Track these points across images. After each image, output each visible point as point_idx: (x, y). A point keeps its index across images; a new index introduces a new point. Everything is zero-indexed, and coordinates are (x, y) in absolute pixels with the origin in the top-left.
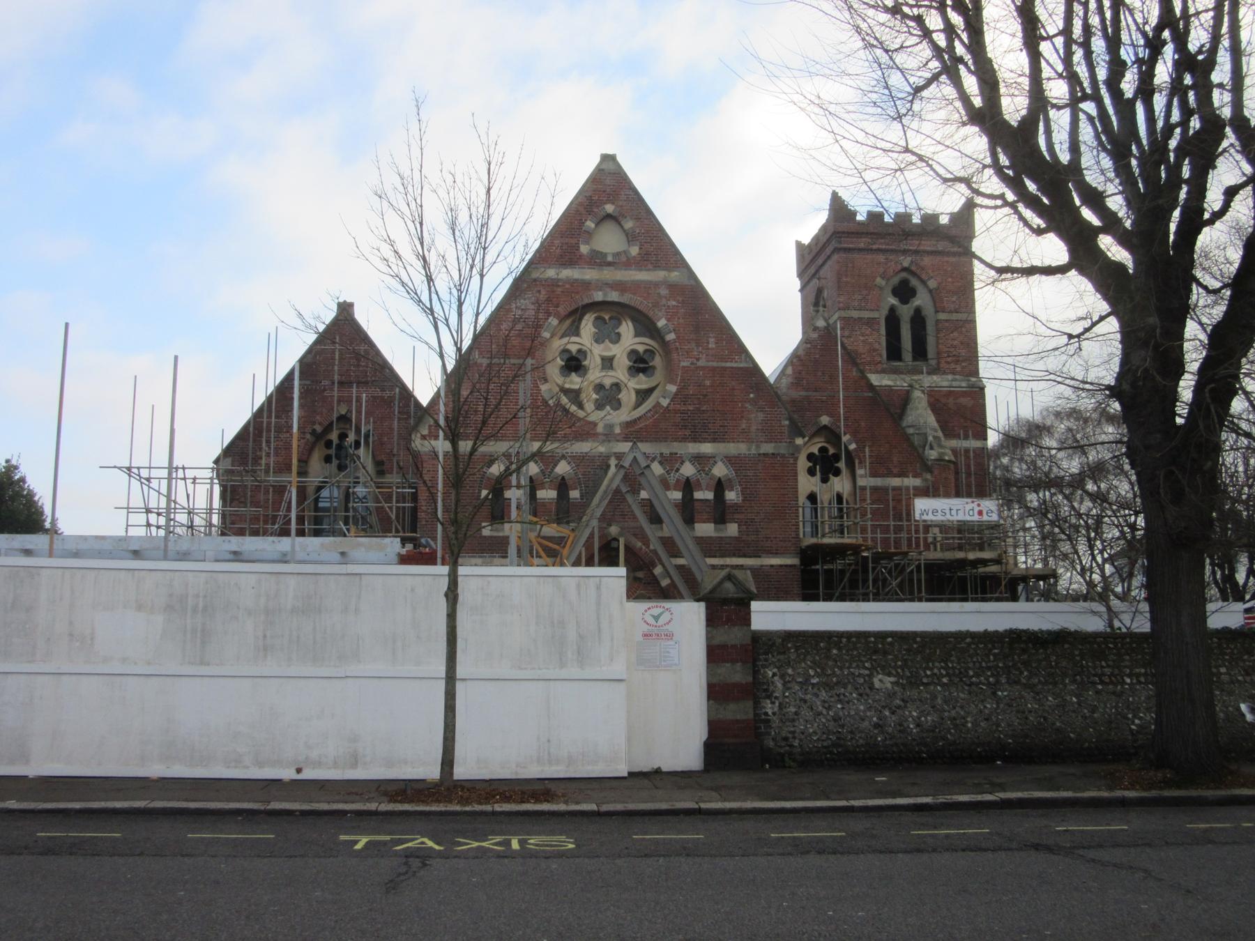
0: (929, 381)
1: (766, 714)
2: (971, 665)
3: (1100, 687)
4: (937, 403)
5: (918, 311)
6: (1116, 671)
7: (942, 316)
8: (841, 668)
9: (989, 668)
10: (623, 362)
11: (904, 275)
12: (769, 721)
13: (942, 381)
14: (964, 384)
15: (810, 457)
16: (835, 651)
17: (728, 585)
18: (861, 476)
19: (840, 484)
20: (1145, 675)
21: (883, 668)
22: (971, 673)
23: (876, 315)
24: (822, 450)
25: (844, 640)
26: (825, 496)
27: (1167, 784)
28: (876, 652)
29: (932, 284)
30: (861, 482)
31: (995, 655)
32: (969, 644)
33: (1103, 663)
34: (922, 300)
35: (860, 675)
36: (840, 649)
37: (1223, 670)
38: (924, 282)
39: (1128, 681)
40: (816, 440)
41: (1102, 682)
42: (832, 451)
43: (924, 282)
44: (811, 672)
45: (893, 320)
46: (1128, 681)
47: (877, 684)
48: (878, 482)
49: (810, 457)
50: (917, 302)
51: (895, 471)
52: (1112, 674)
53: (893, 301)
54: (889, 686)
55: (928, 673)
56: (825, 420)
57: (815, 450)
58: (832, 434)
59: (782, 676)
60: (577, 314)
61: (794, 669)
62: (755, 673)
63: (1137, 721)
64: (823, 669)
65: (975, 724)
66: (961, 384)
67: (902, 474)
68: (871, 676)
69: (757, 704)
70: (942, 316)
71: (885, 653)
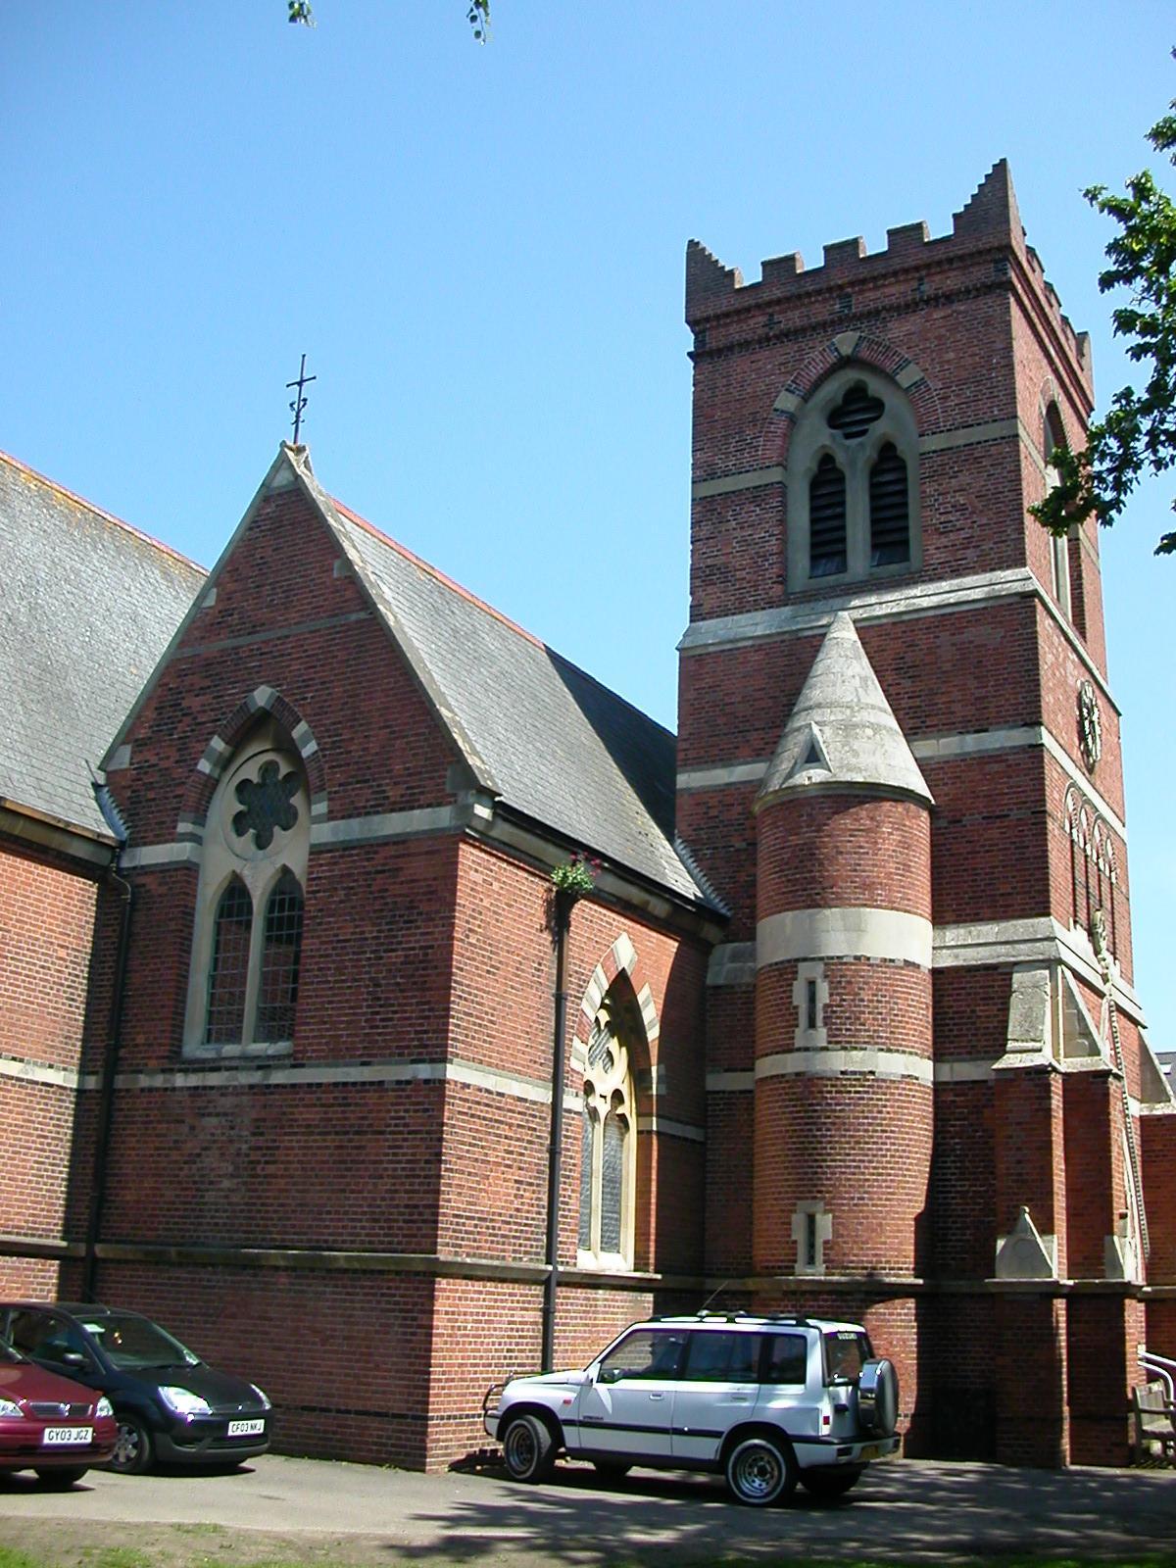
4: (895, 653)
5: (888, 452)
11: (850, 376)
19: (291, 851)
24: (268, 769)
29: (905, 379)
34: (897, 423)
38: (890, 379)
43: (890, 379)
45: (827, 480)
48: (353, 829)
49: (243, 787)
50: (880, 428)
51: (393, 793)
67: (407, 805)
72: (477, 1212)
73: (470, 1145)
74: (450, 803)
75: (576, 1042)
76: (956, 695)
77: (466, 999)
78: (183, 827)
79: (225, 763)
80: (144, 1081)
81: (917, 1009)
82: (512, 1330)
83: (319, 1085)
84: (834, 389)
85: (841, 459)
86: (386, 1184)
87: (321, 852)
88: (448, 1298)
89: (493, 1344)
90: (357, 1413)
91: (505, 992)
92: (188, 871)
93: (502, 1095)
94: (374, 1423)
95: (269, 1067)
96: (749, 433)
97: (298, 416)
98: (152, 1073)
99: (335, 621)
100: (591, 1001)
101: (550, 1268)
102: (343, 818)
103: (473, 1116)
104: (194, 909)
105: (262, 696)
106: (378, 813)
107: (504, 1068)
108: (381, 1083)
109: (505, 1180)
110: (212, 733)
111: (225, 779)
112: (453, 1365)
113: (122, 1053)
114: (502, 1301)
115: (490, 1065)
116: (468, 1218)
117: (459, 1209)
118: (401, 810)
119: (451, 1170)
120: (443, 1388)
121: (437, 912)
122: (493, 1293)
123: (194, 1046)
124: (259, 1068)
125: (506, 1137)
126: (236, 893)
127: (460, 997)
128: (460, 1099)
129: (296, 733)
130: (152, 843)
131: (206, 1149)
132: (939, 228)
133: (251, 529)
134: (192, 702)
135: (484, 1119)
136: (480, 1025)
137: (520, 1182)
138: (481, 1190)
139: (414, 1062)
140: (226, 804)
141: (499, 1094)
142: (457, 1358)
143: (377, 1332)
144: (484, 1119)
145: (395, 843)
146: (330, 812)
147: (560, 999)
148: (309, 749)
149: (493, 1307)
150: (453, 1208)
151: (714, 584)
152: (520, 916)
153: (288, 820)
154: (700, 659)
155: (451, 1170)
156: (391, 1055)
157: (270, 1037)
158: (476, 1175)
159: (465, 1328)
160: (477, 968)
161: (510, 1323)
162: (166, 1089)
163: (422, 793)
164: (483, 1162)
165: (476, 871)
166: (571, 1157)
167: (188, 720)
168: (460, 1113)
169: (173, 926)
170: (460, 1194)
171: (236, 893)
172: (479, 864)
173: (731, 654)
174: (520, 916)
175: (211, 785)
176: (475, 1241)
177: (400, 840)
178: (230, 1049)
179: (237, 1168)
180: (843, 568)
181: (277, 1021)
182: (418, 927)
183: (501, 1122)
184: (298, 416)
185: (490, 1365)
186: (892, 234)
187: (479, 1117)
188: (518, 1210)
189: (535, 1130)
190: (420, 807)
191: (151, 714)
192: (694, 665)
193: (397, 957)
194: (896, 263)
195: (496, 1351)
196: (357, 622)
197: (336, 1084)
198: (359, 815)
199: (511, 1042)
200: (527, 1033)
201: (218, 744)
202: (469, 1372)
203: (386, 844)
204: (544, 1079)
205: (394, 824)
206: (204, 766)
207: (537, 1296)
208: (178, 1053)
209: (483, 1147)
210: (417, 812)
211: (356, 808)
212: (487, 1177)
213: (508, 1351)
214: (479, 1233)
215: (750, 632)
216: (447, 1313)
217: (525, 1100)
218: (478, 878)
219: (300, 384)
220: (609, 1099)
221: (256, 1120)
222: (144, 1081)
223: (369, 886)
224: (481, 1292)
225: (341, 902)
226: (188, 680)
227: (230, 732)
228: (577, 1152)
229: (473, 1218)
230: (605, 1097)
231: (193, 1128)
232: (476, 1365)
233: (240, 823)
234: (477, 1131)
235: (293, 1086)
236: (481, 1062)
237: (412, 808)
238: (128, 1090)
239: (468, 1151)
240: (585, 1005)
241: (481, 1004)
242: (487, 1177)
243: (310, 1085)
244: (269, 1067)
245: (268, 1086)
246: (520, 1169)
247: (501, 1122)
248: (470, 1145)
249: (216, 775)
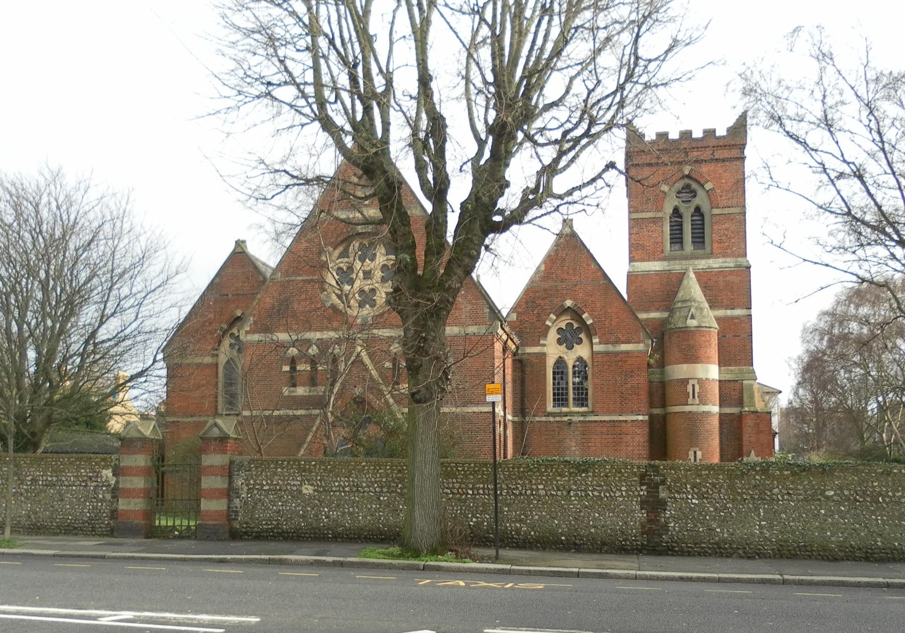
0: (702, 264)
1: (236, 507)
2: (364, 480)
3: (451, 496)
4: (707, 280)
5: (698, 209)
6: (464, 486)
7: (716, 211)
8: (282, 481)
9: (376, 482)
10: (378, 274)
11: (687, 181)
12: (237, 512)
13: (715, 263)
14: (732, 265)
15: (560, 330)
16: (279, 470)
17: (215, 430)
18: (596, 344)
19: (582, 350)
20: (483, 489)
21: (308, 481)
22: (364, 485)
23: (660, 215)
25: (285, 463)
26: (570, 359)
27: (392, 556)
28: (304, 471)
29: (708, 186)
30: (597, 348)
31: (380, 474)
32: (364, 467)
33: (454, 480)
34: (701, 199)
35: (294, 485)
36: (283, 468)
37: (541, 487)
39: (471, 492)
40: (563, 318)
41: (452, 493)
42: (576, 326)
43: (702, 186)
44: (264, 483)
46: (471, 492)
47: (305, 491)
48: (610, 348)
49: (560, 330)
50: (697, 201)
52: (460, 487)
53: (676, 202)
54: (311, 492)
55: (337, 484)
56: (569, 303)
57: (563, 326)
58: (576, 313)
59: (247, 485)
60: (348, 240)
61: (255, 481)
62: (230, 483)
63: (474, 520)
64: (272, 481)
65: (365, 517)
66: (730, 263)
67: (628, 342)
68: (301, 485)
69: (230, 501)
70: (716, 211)
71: (310, 472)
80: (537, 419)
81: (715, 392)
123: (550, 408)
126: (560, 363)
132: (721, 132)
140: (553, 335)
148: (589, 322)
157: (578, 406)
171: (560, 363)
173: (647, 275)
177: (627, 352)
178: (564, 409)
180: (682, 248)
181: (581, 400)
186: (705, 131)
191: (524, 305)
194: (705, 144)
201: (553, 317)
205: (624, 347)
215: (654, 268)
222: (537, 419)
226: (537, 294)
233: (560, 342)
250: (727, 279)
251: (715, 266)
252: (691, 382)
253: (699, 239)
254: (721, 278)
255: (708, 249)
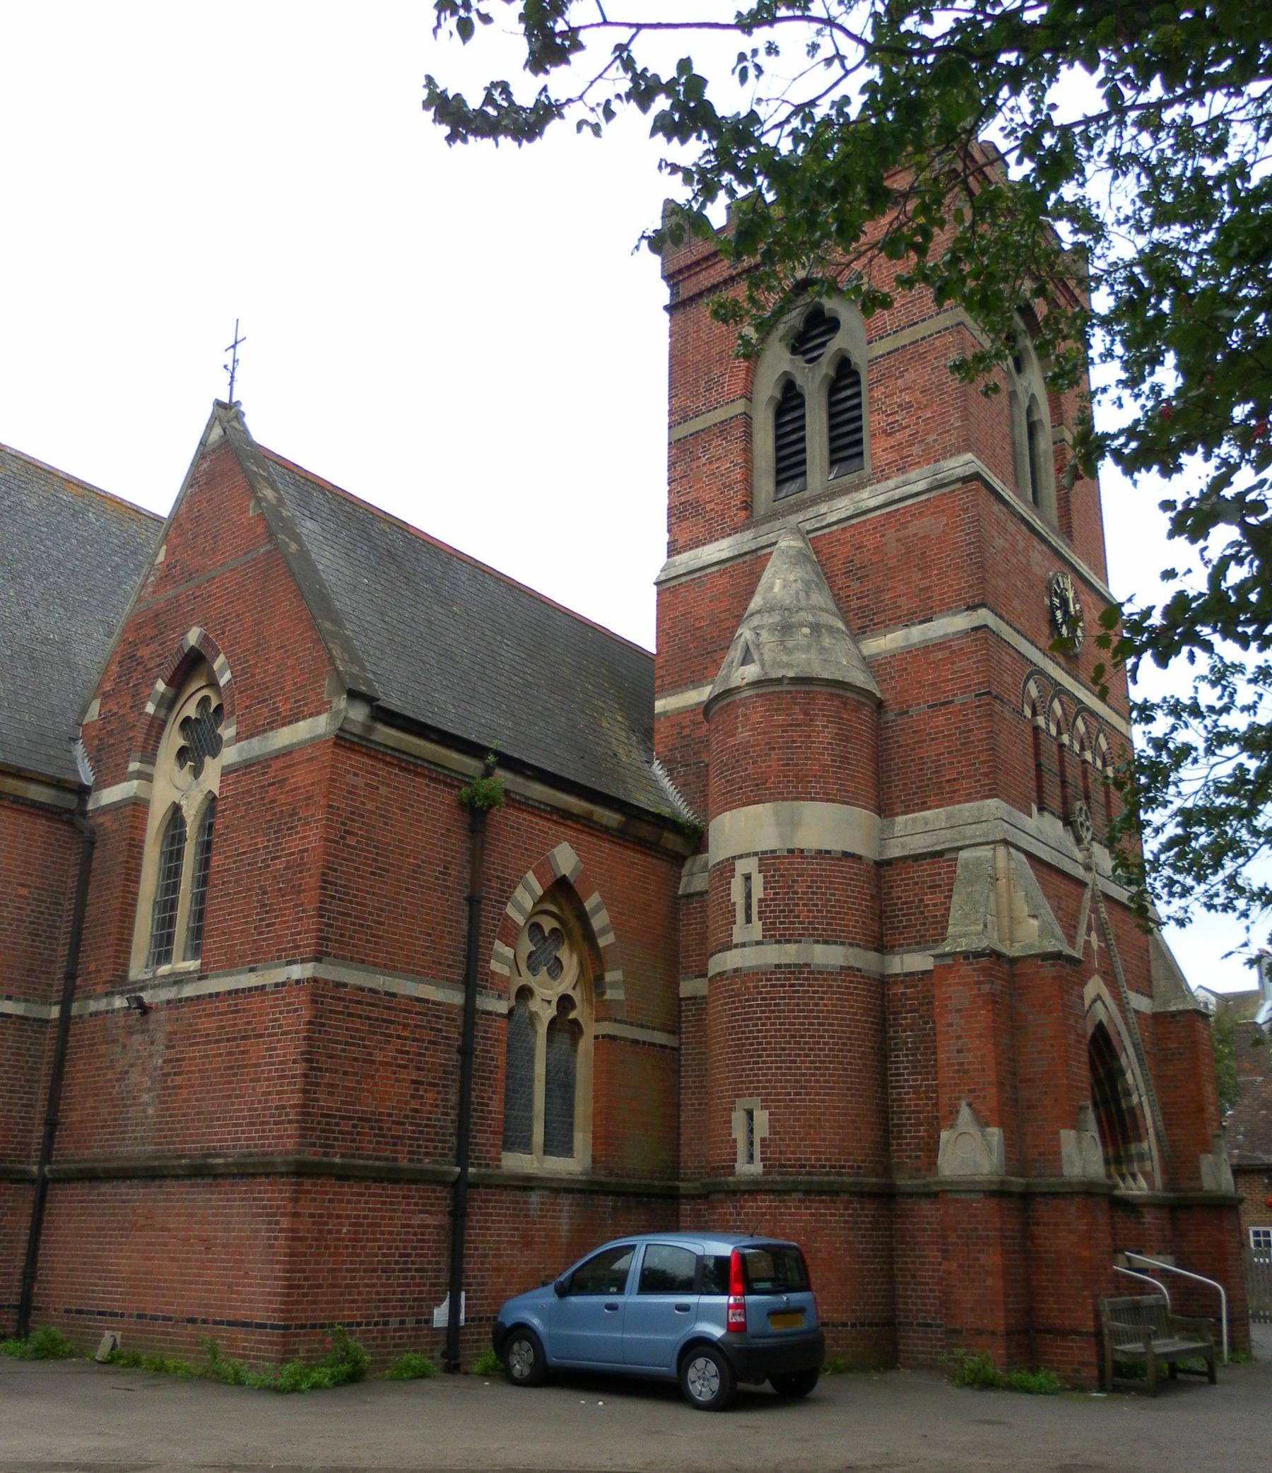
45: (789, 400)
72: (356, 1111)
73: (347, 1043)
74: (326, 710)
75: (499, 946)
76: (902, 589)
77: (340, 899)
78: (134, 766)
79: (169, 703)
80: (93, 1006)
82: (408, 1233)
83: (218, 994)
84: (794, 319)
85: (799, 381)
86: (261, 1087)
87: (230, 773)
88: (314, 1200)
89: (380, 1248)
90: (230, 1323)
91: (398, 893)
92: (138, 806)
93: (394, 995)
94: (240, 1333)
95: (181, 981)
96: (716, 371)
97: (232, 377)
98: (98, 998)
99: (249, 557)
100: (520, 908)
101: (458, 1169)
102: (247, 738)
103: (350, 1015)
104: (143, 841)
105: (193, 637)
106: (272, 729)
107: (395, 968)
108: (264, 986)
109: (397, 1080)
110: (157, 677)
111: (171, 720)
112: (321, 1271)
113: (79, 981)
114: (392, 1203)
115: (375, 964)
116: (343, 1118)
117: (330, 1108)
118: (290, 723)
119: (320, 1070)
120: (305, 1295)
121: (313, 815)
122: (380, 1195)
123: (137, 972)
124: (175, 983)
125: (399, 1037)
127: (333, 897)
128: (332, 998)
129: (216, 666)
130: (110, 785)
131: (132, 1066)
133: (192, 486)
134: (144, 652)
135: (368, 1018)
136: (361, 926)
137: (421, 1083)
138: (362, 1090)
139: (289, 963)
140: (173, 740)
141: (387, 994)
142: (325, 1263)
143: (248, 1238)
144: (368, 1018)
145: (285, 755)
146: (238, 734)
147: (473, 901)
149: (380, 1210)
150: (322, 1108)
151: (687, 520)
152: (417, 821)
153: (215, 747)
154: (674, 591)
155: (320, 1070)
156: (273, 958)
158: (355, 1074)
159: (339, 1232)
160: (357, 869)
161: (404, 1226)
162: (107, 1012)
163: (306, 704)
164: (365, 1061)
165: (356, 775)
166: (492, 1059)
167: (140, 668)
168: (331, 1012)
169: (121, 859)
170: (330, 1094)
172: (361, 769)
174: (417, 821)
175: (157, 728)
176: (353, 1141)
177: (287, 752)
178: (164, 969)
179: (153, 1083)
182: (297, 833)
183: (393, 1022)
184: (232, 377)
185: (375, 1270)
187: (360, 1017)
188: (416, 1111)
189: (440, 1030)
190: (304, 718)
192: (668, 589)
193: (279, 865)
195: (384, 1255)
196: (264, 554)
197: (230, 992)
198: (258, 733)
199: (406, 943)
200: (429, 935)
202: (345, 1278)
203: (277, 757)
204: (453, 981)
206: (150, 708)
207: (445, 1199)
208: (124, 977)
209: (365, 1046)
210: (301, 723)
211: (257, 727)
212: (372, 1077)
213: (401, 1255)
214: (358, 1133)
216: (312, 1216)
217: (427, 1001)
218: (360, 782)
219: (234, 347)
220: (554, 1004)
221: (171, 1033)
222: (93, 1006)
223: (263, 799)
224: (362, 1195)
225: (242, 817)
226: (142, 632)
227: (169, 674)
228: (500, 1054)
229: (351, 1118)
230: (549, 1002)
231: (124, 1046)
232: (353, 1270)
234: (357, 1030)
235: (198, 997)
236: (363, 962)
237: (298, 720)
238: (81, 1016)
239: (344, 1050)
240: (510, 910)
241: (364, 905)
242: (372, 1077)
243: (211, 995)
244: (181, 981)
245: (180, 1000)
246: (419, 1069)
247: (393, 1022)
248: (347, 1043)
249: (162, 714)
250: (911, 530)
251: (872, 503)
252: (742, 867)
253: (846, 447)
254: (890, 533)
255: (868, 469)
